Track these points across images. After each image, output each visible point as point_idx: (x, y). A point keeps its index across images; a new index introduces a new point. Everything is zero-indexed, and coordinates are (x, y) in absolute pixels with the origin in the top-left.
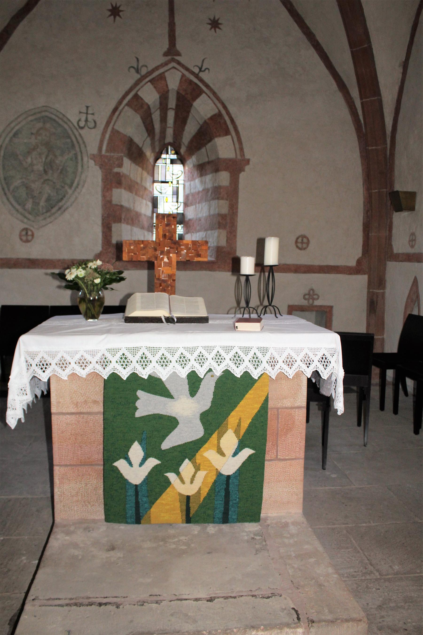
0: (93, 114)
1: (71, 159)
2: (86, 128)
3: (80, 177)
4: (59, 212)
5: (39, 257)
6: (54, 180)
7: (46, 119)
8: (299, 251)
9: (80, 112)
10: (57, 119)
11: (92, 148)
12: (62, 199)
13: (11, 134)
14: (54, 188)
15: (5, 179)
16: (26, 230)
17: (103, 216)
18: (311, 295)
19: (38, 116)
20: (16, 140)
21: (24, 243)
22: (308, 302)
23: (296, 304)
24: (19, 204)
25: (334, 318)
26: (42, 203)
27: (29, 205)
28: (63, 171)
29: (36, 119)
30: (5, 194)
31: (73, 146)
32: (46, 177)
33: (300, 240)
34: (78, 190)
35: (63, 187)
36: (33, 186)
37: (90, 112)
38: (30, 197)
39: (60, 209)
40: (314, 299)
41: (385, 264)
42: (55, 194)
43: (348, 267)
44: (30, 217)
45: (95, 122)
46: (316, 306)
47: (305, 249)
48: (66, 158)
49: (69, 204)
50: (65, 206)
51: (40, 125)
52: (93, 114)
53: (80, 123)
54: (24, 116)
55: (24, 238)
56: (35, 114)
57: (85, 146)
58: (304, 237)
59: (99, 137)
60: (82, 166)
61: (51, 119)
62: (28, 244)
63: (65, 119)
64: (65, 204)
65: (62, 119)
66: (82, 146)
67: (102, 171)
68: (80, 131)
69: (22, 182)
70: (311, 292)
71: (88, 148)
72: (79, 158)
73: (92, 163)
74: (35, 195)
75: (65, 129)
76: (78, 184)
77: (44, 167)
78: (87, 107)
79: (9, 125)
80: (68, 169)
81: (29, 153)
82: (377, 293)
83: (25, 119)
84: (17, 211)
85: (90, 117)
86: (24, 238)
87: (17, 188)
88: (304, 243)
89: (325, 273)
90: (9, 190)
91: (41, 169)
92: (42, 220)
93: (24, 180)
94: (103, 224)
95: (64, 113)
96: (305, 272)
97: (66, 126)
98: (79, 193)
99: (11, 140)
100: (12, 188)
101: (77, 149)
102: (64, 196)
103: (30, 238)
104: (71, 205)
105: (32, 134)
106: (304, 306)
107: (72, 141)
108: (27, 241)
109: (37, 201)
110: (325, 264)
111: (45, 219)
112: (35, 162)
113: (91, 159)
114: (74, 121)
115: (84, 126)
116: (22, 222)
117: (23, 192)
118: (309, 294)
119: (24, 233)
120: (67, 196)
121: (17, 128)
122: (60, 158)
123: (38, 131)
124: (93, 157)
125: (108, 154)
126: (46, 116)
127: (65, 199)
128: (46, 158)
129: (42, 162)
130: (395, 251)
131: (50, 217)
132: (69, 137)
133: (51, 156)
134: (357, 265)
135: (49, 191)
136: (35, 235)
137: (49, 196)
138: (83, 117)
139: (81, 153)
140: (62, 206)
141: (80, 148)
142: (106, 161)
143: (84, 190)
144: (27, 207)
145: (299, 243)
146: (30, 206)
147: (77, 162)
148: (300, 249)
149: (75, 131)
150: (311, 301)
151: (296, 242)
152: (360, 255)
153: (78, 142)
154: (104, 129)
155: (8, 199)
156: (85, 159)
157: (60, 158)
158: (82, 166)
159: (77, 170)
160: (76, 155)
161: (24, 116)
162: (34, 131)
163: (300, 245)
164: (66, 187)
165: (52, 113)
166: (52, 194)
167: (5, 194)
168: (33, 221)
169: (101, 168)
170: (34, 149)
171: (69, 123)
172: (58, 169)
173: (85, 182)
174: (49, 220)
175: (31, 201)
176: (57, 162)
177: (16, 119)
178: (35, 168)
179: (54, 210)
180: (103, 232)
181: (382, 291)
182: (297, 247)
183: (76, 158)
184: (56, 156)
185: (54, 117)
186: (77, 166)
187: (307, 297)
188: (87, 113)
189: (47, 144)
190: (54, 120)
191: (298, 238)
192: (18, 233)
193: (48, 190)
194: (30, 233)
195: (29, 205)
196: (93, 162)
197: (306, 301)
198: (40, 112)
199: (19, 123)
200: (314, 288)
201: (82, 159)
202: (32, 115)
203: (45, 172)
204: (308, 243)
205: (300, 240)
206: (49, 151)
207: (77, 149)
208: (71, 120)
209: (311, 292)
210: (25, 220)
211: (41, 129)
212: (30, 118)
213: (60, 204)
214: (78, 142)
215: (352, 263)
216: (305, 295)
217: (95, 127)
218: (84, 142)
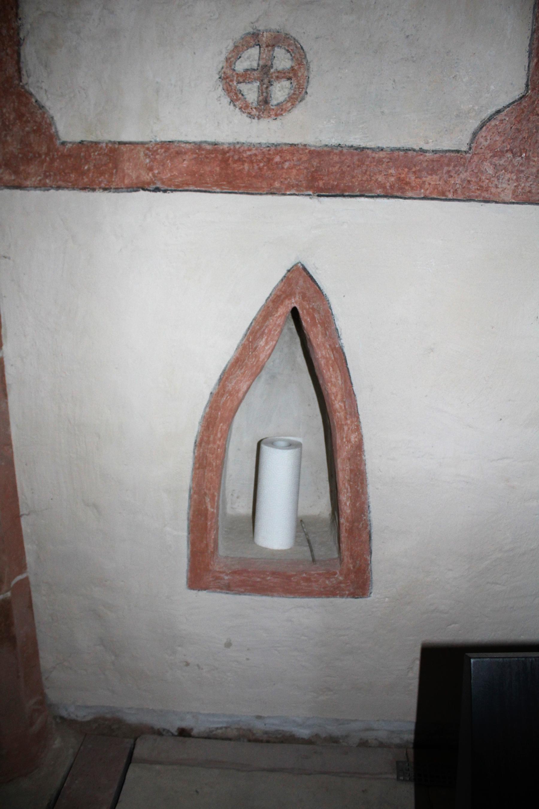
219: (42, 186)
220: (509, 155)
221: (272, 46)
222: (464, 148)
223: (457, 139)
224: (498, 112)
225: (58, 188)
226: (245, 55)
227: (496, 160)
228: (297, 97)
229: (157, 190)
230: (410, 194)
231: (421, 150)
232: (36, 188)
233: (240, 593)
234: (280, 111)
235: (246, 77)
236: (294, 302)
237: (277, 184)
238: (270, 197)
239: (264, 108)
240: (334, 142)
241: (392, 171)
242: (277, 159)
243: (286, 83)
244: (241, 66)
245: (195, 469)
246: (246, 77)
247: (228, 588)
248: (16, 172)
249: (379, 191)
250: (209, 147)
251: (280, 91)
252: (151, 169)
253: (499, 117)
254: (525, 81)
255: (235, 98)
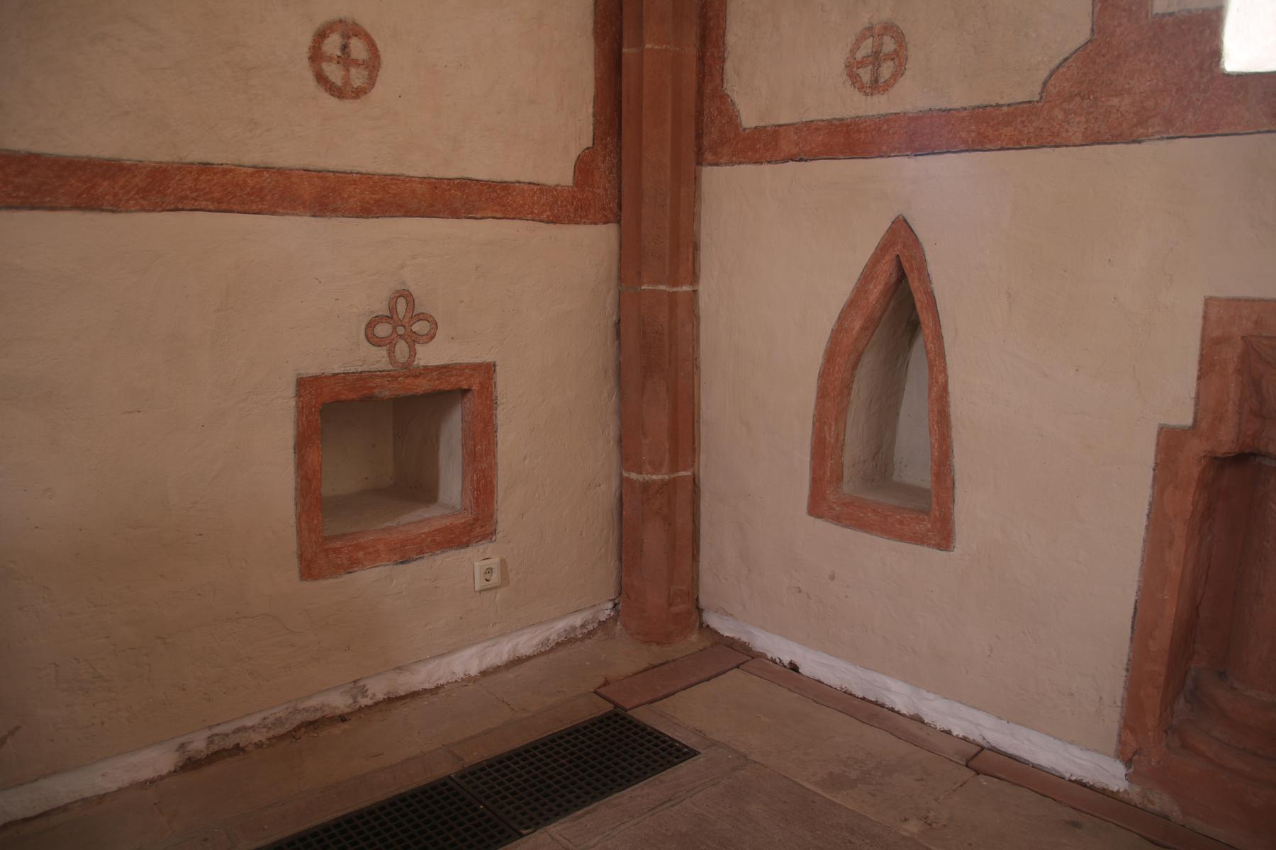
8: (331, 102)
18: (401, 318)
22: (391, 353)
23: (336, 367)
25: (501, 415)
33: (332, 45)
40: (413, 340)
41: (696, 179)
43: (542, 189)
46: (427, 369)
47: (359, 93)
58: (350, 30)
70: (402, 305)
82: (672, 296)
88: (356, 63)
89: (455, 214)
96: (365, 212)
106: (372, 375)
110: (452, 173)
118: (390, 317)
130: (749, 118)
134: (576, 184)
145: (330, 59)
148: (338, 92)
150: (402, 348)
151: (316, 56)
152: (587, 141)
163: (334, 73)
181: (686, 288)
182: (321, 78)
187: (383, 330)
191: (321, 35)
197: (383, 352)
200: (413, 288)
204: (373, 64)
205: (332, 45)
209: (402, 305)
215: (560, 173)
216: (371, 325)
219: (731, 163)
220: (1078, 99)
221: (881, 35)
222: (1036, 98)
223: (1027, 91)
224: (1066, 60)
225: (740, 163)
226: (862, 47)
227: (1065, 105)
228: (898, 74)
229: (801, 160)
230: (989, 147)
231: (998, 105)
232: (726, 164)
233: (846, 526)
234: (888, 85)
235: (861, 64)
236: (897, 250)
237: (884, 148)
238: (879, 160)
239: (876, 87)
240: (927, 107)
241: (973, 127)
242: (885, 127)
243: (890, 63)
244: (859, 56)
245: (818, 398)
246: (861, 64)
247: (837, 519)
248: (715, 153)
249: (962, 147)
250: (837, 123)
251: (886, 70)
252: (797, 144)
253: (1066, 64)
254: (1089, 26)
255: (854, 78)
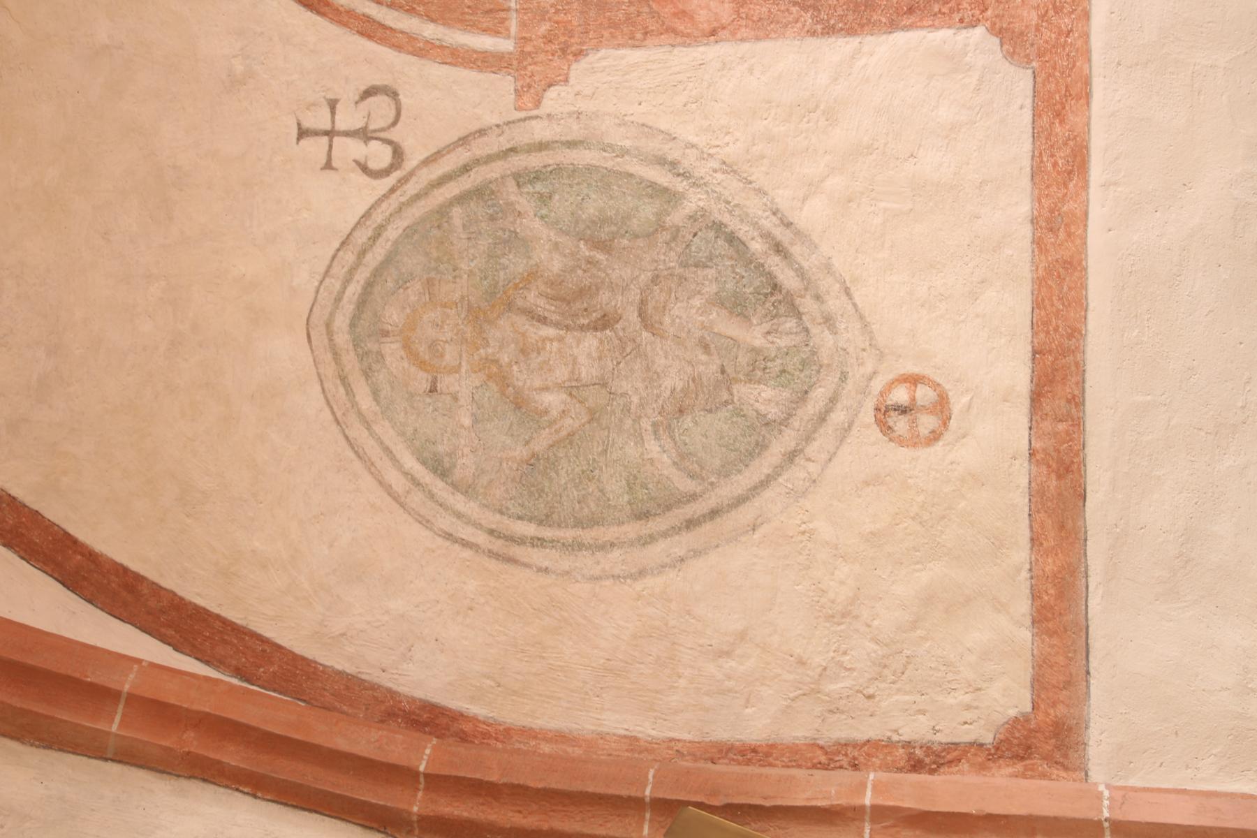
0: (333, 105)
1: (544, 199)
2: (393, 135)
3: (624, 152)
4: (796, 250)
5: (1025, 351)
6: (644, 278)
7: (367, 328)
9: (328, 166)
10: (362, 275)
11: (484, 99)
12: (732, 239)
13: (439, 487)
14: (683, 279)
15: (643, 516)
16: (884, 412)
17: (813, 33)
19: (349, 359)
20: (466, 466)
21: (953, 423)
24: (762, 446)
26: (755, 336)
27: (763, 398)
28: (601, 237)
29: (367, 374)
30: (714, 513)
31: (479, 193)
32: (633, 316)
34: (689, 160)
35: (676, 232)
36: (673, 381)
37: (321, 120)
38: (725, 396)
39: (778, 248)
42: (711, 273)
44: (819, 395)
45: (369, 93)
48: (537, 224)
49: (754, 206)
50: (769, 223)
51: (392, 350)
52: (333, 105)
53: (373, 165)
54: (357, 432)
55: (927, 423)
56: (343, 379)
57: (482, 132)
59: (437, 71)
60: (571, 144)
61: (362, 303)
62: (958, 404)
63: (362, 237)
64: (755, 225)
65: (363, 253)
66: (480, 148)
67: (597, 48)
68: (409, 164)
69: (657, 438)
71: (491, 119)
72: (535, 161)
73: (554, 100)
74: (714, 368)
75: (409, 232)
76: (661, 161)
77: (582, 328)
78: (303, 133)
79: (396, 498)
80: (591, 210)
81: (519, 403)
83: (368, 426)
84: (792, 456)
85: (346, 120)
86: (927, 423)
87: (683, 458)
90: (693, 497)
91: (590, 342)
92: (833, 330)
93: (646, 424)
94: (850, 32)
95: (336, 245)
97: (392, 233)
98: (704, 157)
99: (466, 489)
100: (687, 485)
101: (494, 171)
102: (718, 227)
103: (924, 394)
104: (761, 192)
105: (433, 390)
107: (461, 199)
108: (942, 406)
109: (743, 359)
111: (828, 321)
112: (561, 373)
113: (538, 104)
114: (365, 192)
115: (390, 142)
116: (847, 429)
117: (703, 430)
119: (901, 424)
120: (717, 216)
121: (410, 463)
122: (541, 254)
123: (413, 356)
124: (530, 92)
125: (513, 26)
126: (352, 325)
127: (733, 224)
128: (543, 320)
129: (561, 339)
131: (818, 298)
132: (443, 212)
133: (532, 298)
135: (697, 302)
136: (911, 368)
137: (718, 301)
138: (350, 149)
139: (513, 150)
140: (766, 236)
141: (489, 159)
142: (544, 28)
143: (688, 133)
144: (773, 412)
146: (767, 393)
147: (559, 169)
149: (411, 188)
153: (466, 169)
154: (398, 47)
155: (740, 501)
156: (541, 131)
157: (541, 254)
158: (571, 144)
159: (590, 169)
160: (520, 178)
161: (357, 432)
162: (421, 381)
164: (676, 217)
165: (338, 299)
166: (714, 288)
167: (714, 513)
168: (844, 377)
169: (579, 54)
170: (503, 380)
171: (378, 218)
172: (590, 261)
173: (646, 129)
174: (835, 303)
175: (743, 391)
176: (556, 265)
177: (370, 465)
178: (588, 371)
179: (788, 279)
180: (893, 26)
183: (537, 176)
184: (532, 276)
185: (354, 289)
186: (574, 171)
188: (330, 133)
189: (479, 316)
190: (369, 285)
192: (904, 452)
193: (688, 312)
194: (900, 395)
195: (763, 398)
196: (552, 93)
198: (336, 356)
199: (387, 450)
201: (542, 146)
202: (349, 391)
203: (605, 322)
206: (510, 306)
207: (494, 171)
208: (361, 210)
210: (838, 417)
211: (406, 346)
212: (365, 401)
213: (757, 246)
214: (466, 169)
217: (394, 95)
218: (464, 141)
